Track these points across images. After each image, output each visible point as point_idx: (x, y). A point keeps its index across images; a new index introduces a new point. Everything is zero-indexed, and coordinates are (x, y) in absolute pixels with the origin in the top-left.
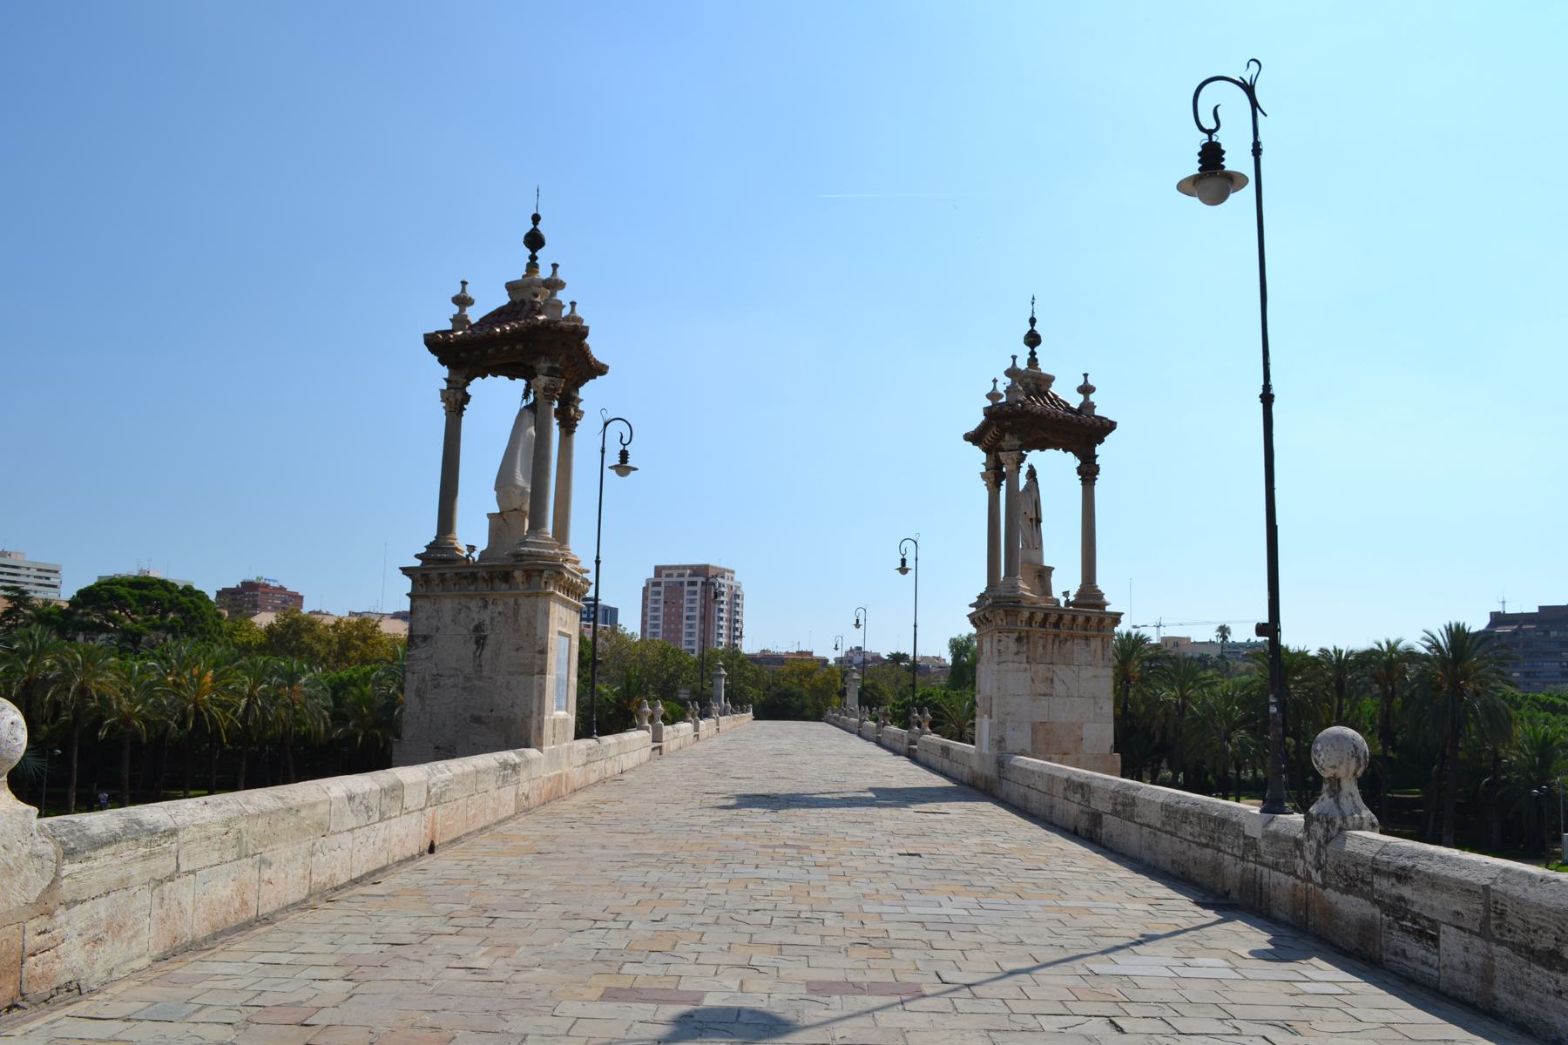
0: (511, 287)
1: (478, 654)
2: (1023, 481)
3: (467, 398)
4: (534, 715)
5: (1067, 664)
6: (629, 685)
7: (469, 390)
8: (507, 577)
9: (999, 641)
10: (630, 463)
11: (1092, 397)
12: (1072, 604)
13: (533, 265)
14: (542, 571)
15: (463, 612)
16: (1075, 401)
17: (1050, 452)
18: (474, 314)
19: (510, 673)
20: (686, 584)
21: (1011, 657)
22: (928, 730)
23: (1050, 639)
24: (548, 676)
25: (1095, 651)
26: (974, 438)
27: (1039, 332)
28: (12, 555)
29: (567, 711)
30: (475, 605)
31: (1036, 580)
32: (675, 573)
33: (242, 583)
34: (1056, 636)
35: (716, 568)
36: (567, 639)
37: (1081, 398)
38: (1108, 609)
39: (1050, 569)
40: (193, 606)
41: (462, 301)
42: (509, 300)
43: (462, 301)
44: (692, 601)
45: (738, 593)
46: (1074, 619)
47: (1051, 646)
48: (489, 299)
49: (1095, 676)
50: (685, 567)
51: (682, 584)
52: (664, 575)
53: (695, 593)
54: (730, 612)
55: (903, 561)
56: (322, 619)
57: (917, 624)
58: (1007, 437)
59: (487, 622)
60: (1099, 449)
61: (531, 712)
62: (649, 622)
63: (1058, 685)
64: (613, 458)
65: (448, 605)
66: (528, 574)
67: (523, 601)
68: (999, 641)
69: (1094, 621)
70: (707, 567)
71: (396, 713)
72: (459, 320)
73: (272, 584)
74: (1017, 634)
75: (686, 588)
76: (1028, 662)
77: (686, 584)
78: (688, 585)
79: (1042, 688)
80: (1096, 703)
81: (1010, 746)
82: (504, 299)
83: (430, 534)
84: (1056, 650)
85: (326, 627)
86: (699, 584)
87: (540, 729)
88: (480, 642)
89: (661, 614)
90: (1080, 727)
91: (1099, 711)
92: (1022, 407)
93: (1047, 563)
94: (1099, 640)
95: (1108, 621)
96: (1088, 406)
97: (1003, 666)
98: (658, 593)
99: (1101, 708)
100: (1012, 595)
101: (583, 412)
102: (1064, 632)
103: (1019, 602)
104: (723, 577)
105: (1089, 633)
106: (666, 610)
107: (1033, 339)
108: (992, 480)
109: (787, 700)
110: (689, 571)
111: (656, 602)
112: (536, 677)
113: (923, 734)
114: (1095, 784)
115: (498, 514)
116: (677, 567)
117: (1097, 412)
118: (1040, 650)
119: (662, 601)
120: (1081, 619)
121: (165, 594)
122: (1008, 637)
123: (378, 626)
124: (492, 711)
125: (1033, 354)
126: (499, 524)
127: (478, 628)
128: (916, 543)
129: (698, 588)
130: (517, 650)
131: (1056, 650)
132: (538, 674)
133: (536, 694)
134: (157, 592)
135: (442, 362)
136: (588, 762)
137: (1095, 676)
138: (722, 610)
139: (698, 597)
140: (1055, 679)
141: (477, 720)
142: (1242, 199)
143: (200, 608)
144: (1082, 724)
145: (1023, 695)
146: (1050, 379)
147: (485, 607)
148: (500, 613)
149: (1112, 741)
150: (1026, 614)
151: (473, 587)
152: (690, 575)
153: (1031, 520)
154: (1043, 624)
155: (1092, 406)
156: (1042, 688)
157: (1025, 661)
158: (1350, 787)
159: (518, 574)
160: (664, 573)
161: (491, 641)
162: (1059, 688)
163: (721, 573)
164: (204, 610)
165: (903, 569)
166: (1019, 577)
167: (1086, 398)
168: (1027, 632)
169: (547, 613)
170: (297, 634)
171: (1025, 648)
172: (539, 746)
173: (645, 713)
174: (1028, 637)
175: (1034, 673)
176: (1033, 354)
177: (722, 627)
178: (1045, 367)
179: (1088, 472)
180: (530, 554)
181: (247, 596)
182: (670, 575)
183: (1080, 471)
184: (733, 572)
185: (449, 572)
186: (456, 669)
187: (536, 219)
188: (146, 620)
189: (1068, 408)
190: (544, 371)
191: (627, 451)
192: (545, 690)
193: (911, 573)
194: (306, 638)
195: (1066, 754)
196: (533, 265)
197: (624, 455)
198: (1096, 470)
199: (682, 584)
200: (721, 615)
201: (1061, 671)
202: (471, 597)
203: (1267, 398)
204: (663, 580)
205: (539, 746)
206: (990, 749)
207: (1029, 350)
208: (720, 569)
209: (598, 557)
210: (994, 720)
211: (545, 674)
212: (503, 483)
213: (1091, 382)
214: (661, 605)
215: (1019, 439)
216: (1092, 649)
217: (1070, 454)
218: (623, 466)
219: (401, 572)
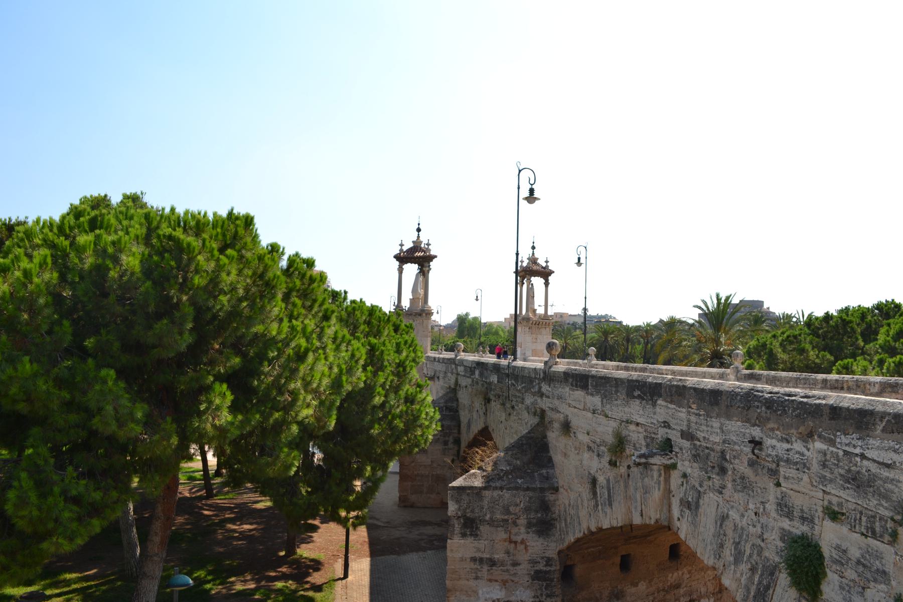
0: (413, 242)
8: (420, 315)
11: (548, 264)
13: (418, 237)
16: (544, 265)
18: (405, 248)
41: (402, 245)
43: (402, 245)
48: (408, 245)
60: (550, 278)
66: (426, 314)
72: (401, 250)
79: (535, 341)
81: (527, 355)
82: (412, 245)
96: (547, 266)
102: (540, 326)
117: (550, 268)
126: (413, 301)
142: (583, 266)
146: (537, 259)
154: (535, 324)
156: (535, 341)
158: (593, 356)
159: (424, 315)
162: (539, 341)
165: (477, 300)
178: (536, 256)
179: (547, 284)
183: (544, 283)
187: (419, 224)
189: (542, 267)
196: (418, 237)
201: (539, 336)
203: (586, 298)
212: (414, 290)
213: (548, 260)
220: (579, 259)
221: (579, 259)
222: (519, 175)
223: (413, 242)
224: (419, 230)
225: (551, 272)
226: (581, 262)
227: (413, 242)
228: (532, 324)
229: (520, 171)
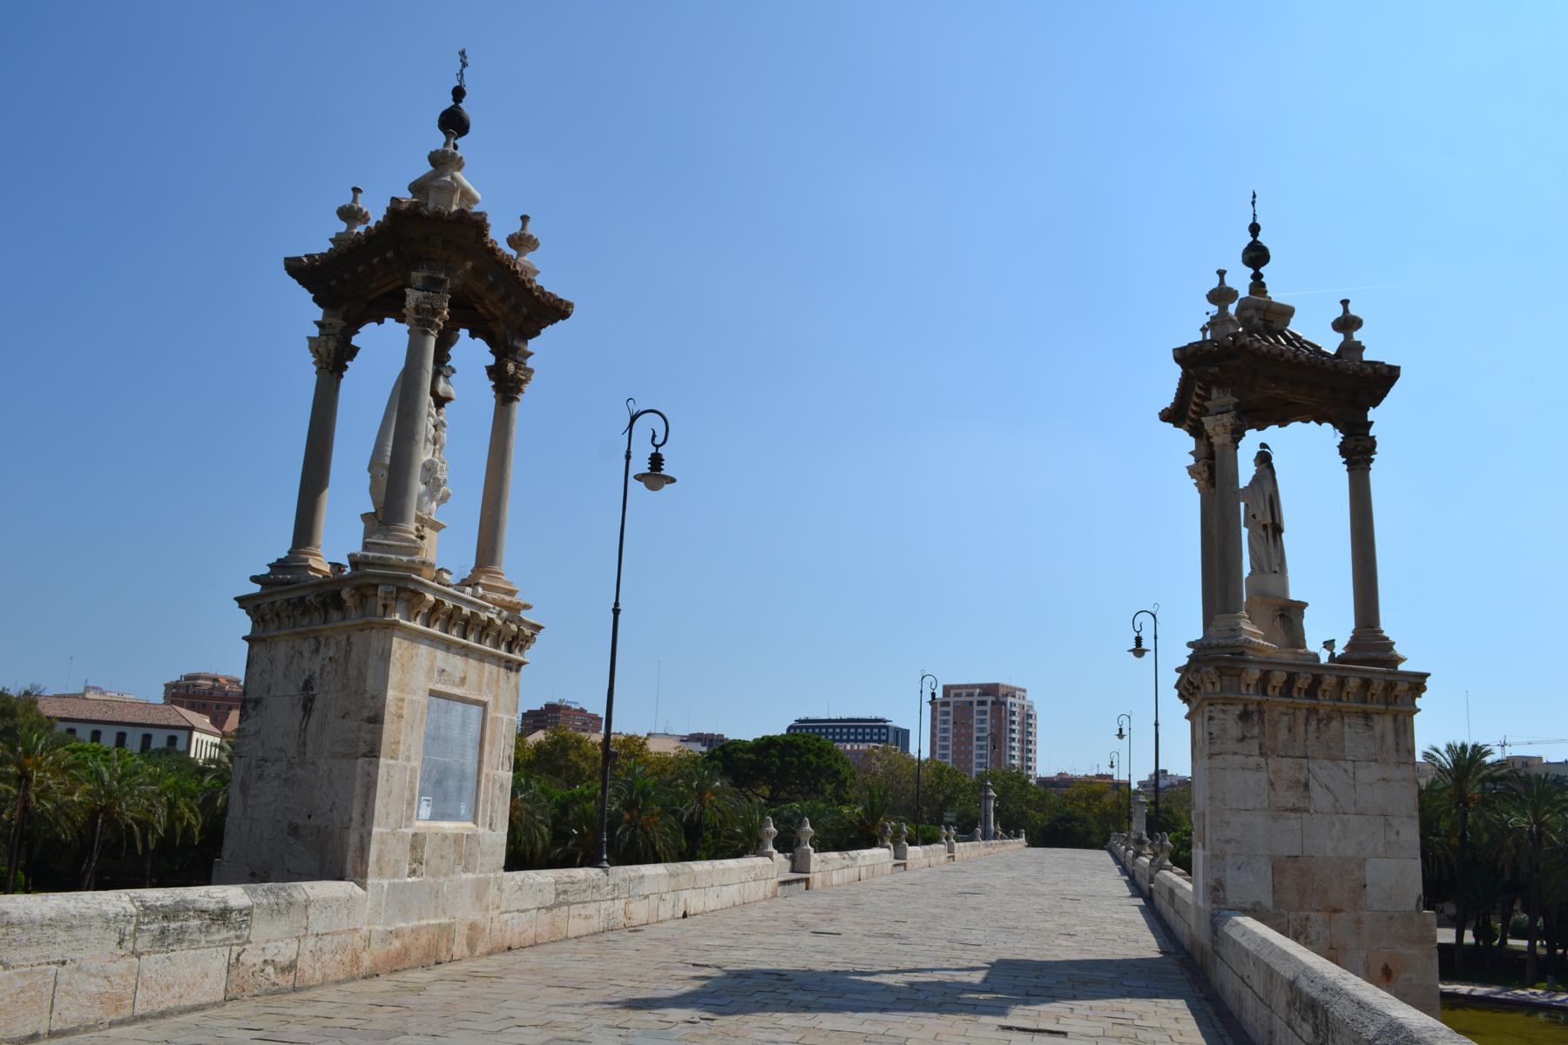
1: (304, 726)
2: (1246, 471)
3: (354, 351)
4: (355, 825)
5: (1333, 759)
6: (873, 805)
7: (356, 341)
9: (1211, 718)
10: (667, 470)
11: (1357, 336)
12: (1341, 659)
14: (376, 586)
15: (295, 659)
16: (1330, 342)
17: (1296, 427)
20: (975, 703)
21: (1231, 746)
22: (1168, 863)
23: (1301, 716)
24: (382, 761)
25: (1383, 737)
26: (1172, 415)
27: (1265, 244)
29: (475, 822)
30: (307, 646)
31: (1277, 623)
32: (964, 692)
33: (546, 705)
34: (1312, 711)
35: (1007, 687)
36: (481, 708)
37: (1340, 337)
38: (1402, 667)
39: (1301, 606)
44: (982, 721)
45: (1030, 713)
46: (1342, 683)
47: (1303, 727)
49: (1384, 779)
50: (974, 686)
51: (971, 703)
52: (952, 695)
53: (985, 713)
54: (1022, 732)
55: (1138, 640)
56: (589, 738)
57: (1159, 722)
58: (1214, 393)
61: (351, 819)
62: (938, 743)
63: (1316, 790)
64: (641, 465)
67: (356, 638)
68: (1211, 718)
69: (1378, 686)
70: (996, 686)
71: (618, 833)
73: (573, 706)
74: (1240, 707)
75: (976, 708)
76: (1262, 754)
77: (975, 703)
78: (978, 705)
79: (1289, 798)
80: (1388, 825)
83: (281, 547)
84: (1312, 736)
85: (594, 744)
86: (989, 703)
87: (363, 850)
89: (950, 735)
90: (1361, 864)
91: (1392, 837)
92: (1234, 342)
93: (1294, 594)
94: (1389, 719)
95: (1402, 687)
96: (1351, 349)
97: (1218, 761)
98: (947, 713)
99: (1398, 833)
100: (1230, 642)
101: (531, 371)
102: (1325, 703)
103: (1242, 653)
104: (1014, 696)
105: (1370, 707)
106: (955, 731)
107: (1256, 256)
108: (1205, 475)
109: (1069, 825)
110: (978, 690)
111: (945, 722)
112: (360, 761)
113: (1161, 869)
114: (1339, 1010)
115: (372, 513)
116: (966, 686)
117: (1367, 356)
118: (1283, 735)
119: (951, 723)
120: (1353, 683)
122: (1223, 711)
123: (645, 745)
124: (309, 817)
125: (1257, 277)
127: (307, 686)
128: (1154, 616)
129: (988, 708)
130: (343, 717)
131: (1312, 736)
132: (365, 755)
133: (358, 789)
135: (318, 300)
136: (558, 905)
137: (1384, 779)
138: (1014, 731)
139: (988, 717)
140: (1313, 784)
141: (294, 830)
144: (1365, 859)
145: (1254, 809)
146: (1287, 312)
147: (317, 650)
148: (330, 658)
149: (1419, 889)
150: (1254, 673)
151: (306, 621)
152: (979, 695)
153: (1265, 527)
154: (1288, 688)
155: (1359, 348)
156: (1289, 798)
157: (1257, 752)
159: (345, 594)
160: (953, 692)
161: (317, 705)
162: (1320, 799)
163: (1012, 692)
165: (1139, 651)
166: (1244, 613)
167: (1348, 337)
168: (1259, 703)
169: (385, 657)
170: (565, 751)
171: (1256, 730)
172: (360, 878)
173: (769, 834)
174: (1261, 713)
175: (1274, 772)
176: (1257, 277)
177: (1014, 749)
178: (1277, 293)
181: (549, 718)
182: (959, 695)
183: (1344, 449)
184: (1024, 691)
186: (281, 750)
190: (419, 284)
191: (660, 455)
192: (375, 783)
193: (1149, 656)
194: (573, 756)
195: (1336, 911)
197: (656, 461)
198: (1371, 445)
199: (971, 703)
200: (1013, 735)
201: (1323, 771)
202: (303, 636)
204: (952, 699)
205: (360, 878)
206: (1204, 903)
207: (1251, 271)
208: (1011, 688)
209: (617, 604)
210: (1208, 853)
211: (378, 757)
213: (1354, 310)
214: (950, 726)
215: (1233, 395)
216: (1378, 729)
217: (1328, 427)
218: (656, 474)
219: (237, 604)
225: (1384, 378)
228: (1264, 682)
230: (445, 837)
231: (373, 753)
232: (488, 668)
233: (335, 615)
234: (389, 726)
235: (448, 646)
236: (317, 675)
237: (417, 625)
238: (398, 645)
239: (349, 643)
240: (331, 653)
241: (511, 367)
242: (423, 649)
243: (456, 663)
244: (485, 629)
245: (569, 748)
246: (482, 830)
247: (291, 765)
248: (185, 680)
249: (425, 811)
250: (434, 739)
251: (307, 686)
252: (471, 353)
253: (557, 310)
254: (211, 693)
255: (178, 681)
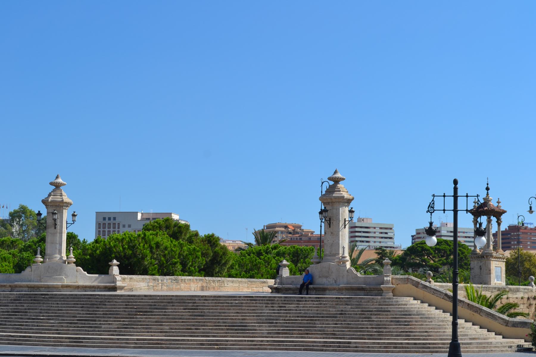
13: (488, 194)
14: (488, 256)
19: (485, 274)
24: (491, 275)
28: (365, 220)
29: (501, 281)
30: (480, 262)
40: (461, 252)
42: (484, 201)
59: (482, 265)
65: (476, 262)
73: (529, 226)
88: (481, 269)
121: (447, 247)
127: (480, 266)
133: (489, 278)
134: (444, 246)
143: (464, 253)
147: (481, 262)
159: (485, 256)
161: (482, 268)
164: (466, 254)
169: (490, 263)
170: (522, 262)
180: (487, 253)
185: (475, 256)
187: (488, 184)
188: (439, 261)
194: (527, 265)
196: (488, 194)
202: (479, 261)
220: (531, 208)
221: (531, 208)
222: (322, 185)
223: (483, 199)
224: (488, 189)
226: (533, 210)
227: (483, 199)
229: (322, 183)
230: (498, 283)
231: (490, 274)
232: (501, 262)
233: (483, 259)
234: (491, 271)
235: (496, 261)
236: (482, 265)
237: (493, 259)
238: (491, 262)
239: (486, 262)
240: (483, 263)
241: (499, 221)
242: (494, 262)
243: (497, 263)
244: (500, 258)
245: (525, 261)
246: (502, 283)
247: (479, 276)
248: (267, 229)
249: (496, 280)
250: (496, 272)
251: (480, 266)
252: (494, 219)
253: (504, 212)
254: (301, 239)
255: (263, 230)
